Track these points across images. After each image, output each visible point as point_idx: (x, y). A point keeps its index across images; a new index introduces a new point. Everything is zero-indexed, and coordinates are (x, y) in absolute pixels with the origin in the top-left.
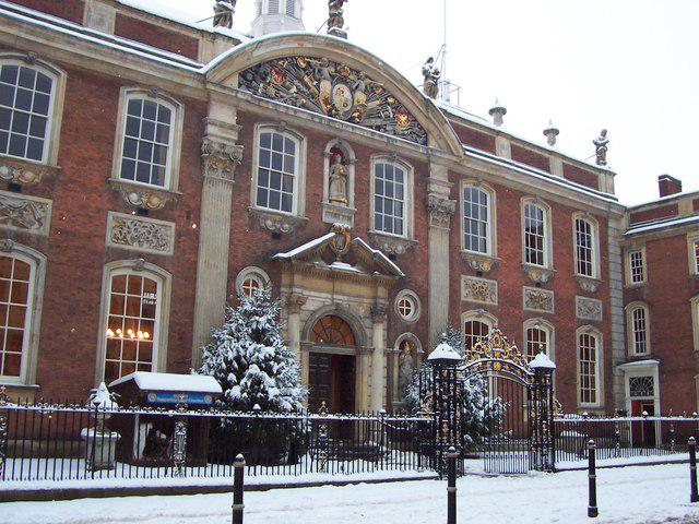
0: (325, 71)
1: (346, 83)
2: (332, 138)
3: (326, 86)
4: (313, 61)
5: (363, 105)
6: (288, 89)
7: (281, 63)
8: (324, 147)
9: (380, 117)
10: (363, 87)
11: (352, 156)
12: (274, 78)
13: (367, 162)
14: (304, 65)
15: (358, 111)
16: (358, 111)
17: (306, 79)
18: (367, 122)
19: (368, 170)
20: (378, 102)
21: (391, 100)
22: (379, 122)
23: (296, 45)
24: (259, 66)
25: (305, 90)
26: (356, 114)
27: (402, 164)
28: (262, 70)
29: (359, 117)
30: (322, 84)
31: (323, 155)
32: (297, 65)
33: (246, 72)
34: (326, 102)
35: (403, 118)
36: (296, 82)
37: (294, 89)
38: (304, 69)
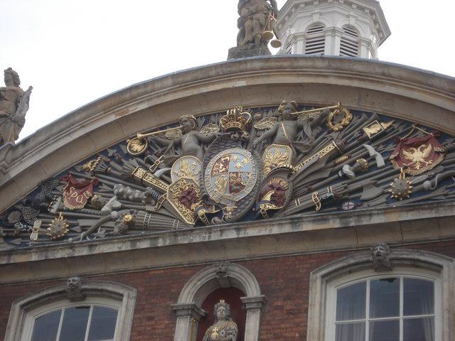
0: (189, 141)
1: (245, 143)
2: (195, 268)
3: (186, 169)
4: (170, 132)
5: (288, 172)
6: (99, 206)
7: (89, 165)
8: (178, 294)
9: (345, 177)
10: (285, 129)
11: (253, 290)
12: (71, 199)
13: (301, 290)
14: (138, 148)
15: (272, 187)
16: (272, 187)
17: (140, 173)
18: (299, 203)
19: (301, 311)
20: (329, 148)
21: (371, 131)
22: (329, 192)
23: (112, 118)
24: (39, 189)
25: (137, 194)
26: (268, 197)
27: (416, 264)
28: (41, 196)
29: (272, 201)
30: (175, 170)
31: (174, 314)
32: (128, 156)
33: (13, 209)
34: (188, 198)
35: (417, 156)
36: (119, 188)
37: (114, 202)
38: (142, 156)
